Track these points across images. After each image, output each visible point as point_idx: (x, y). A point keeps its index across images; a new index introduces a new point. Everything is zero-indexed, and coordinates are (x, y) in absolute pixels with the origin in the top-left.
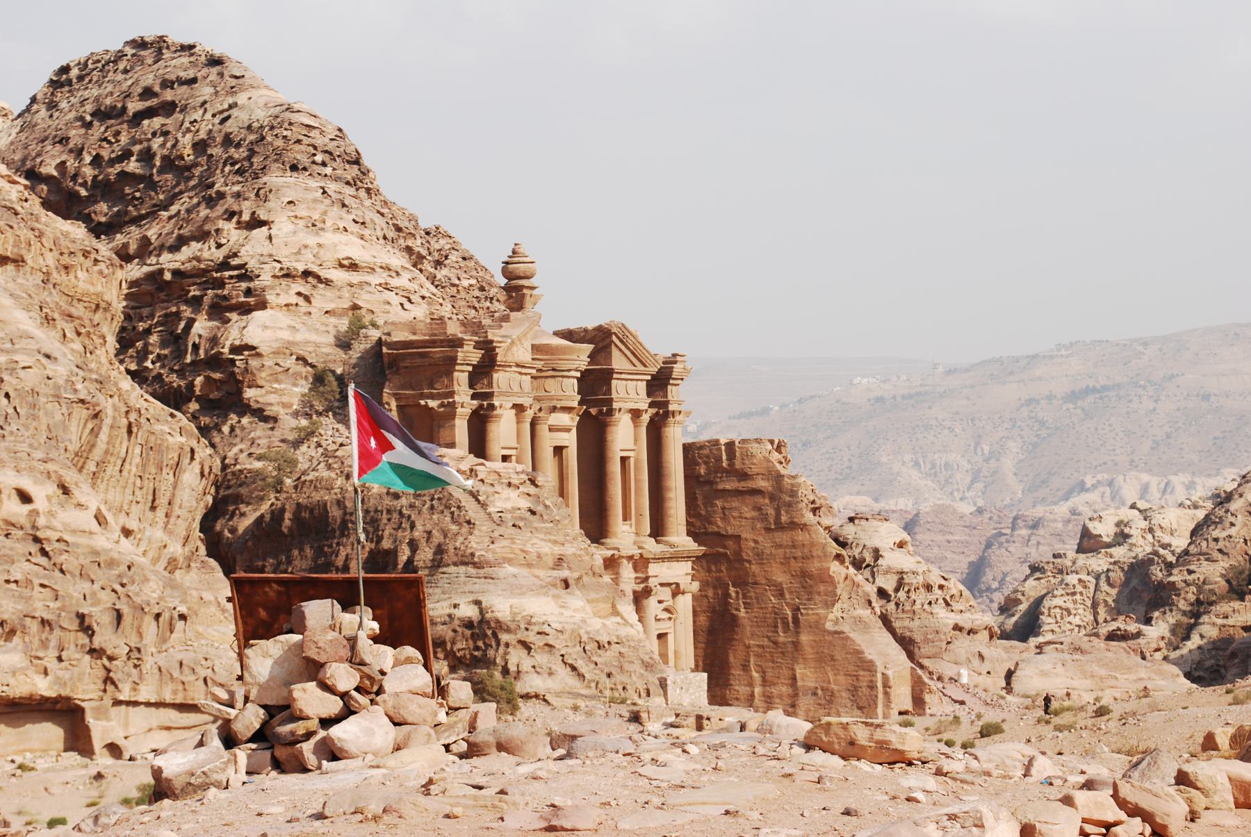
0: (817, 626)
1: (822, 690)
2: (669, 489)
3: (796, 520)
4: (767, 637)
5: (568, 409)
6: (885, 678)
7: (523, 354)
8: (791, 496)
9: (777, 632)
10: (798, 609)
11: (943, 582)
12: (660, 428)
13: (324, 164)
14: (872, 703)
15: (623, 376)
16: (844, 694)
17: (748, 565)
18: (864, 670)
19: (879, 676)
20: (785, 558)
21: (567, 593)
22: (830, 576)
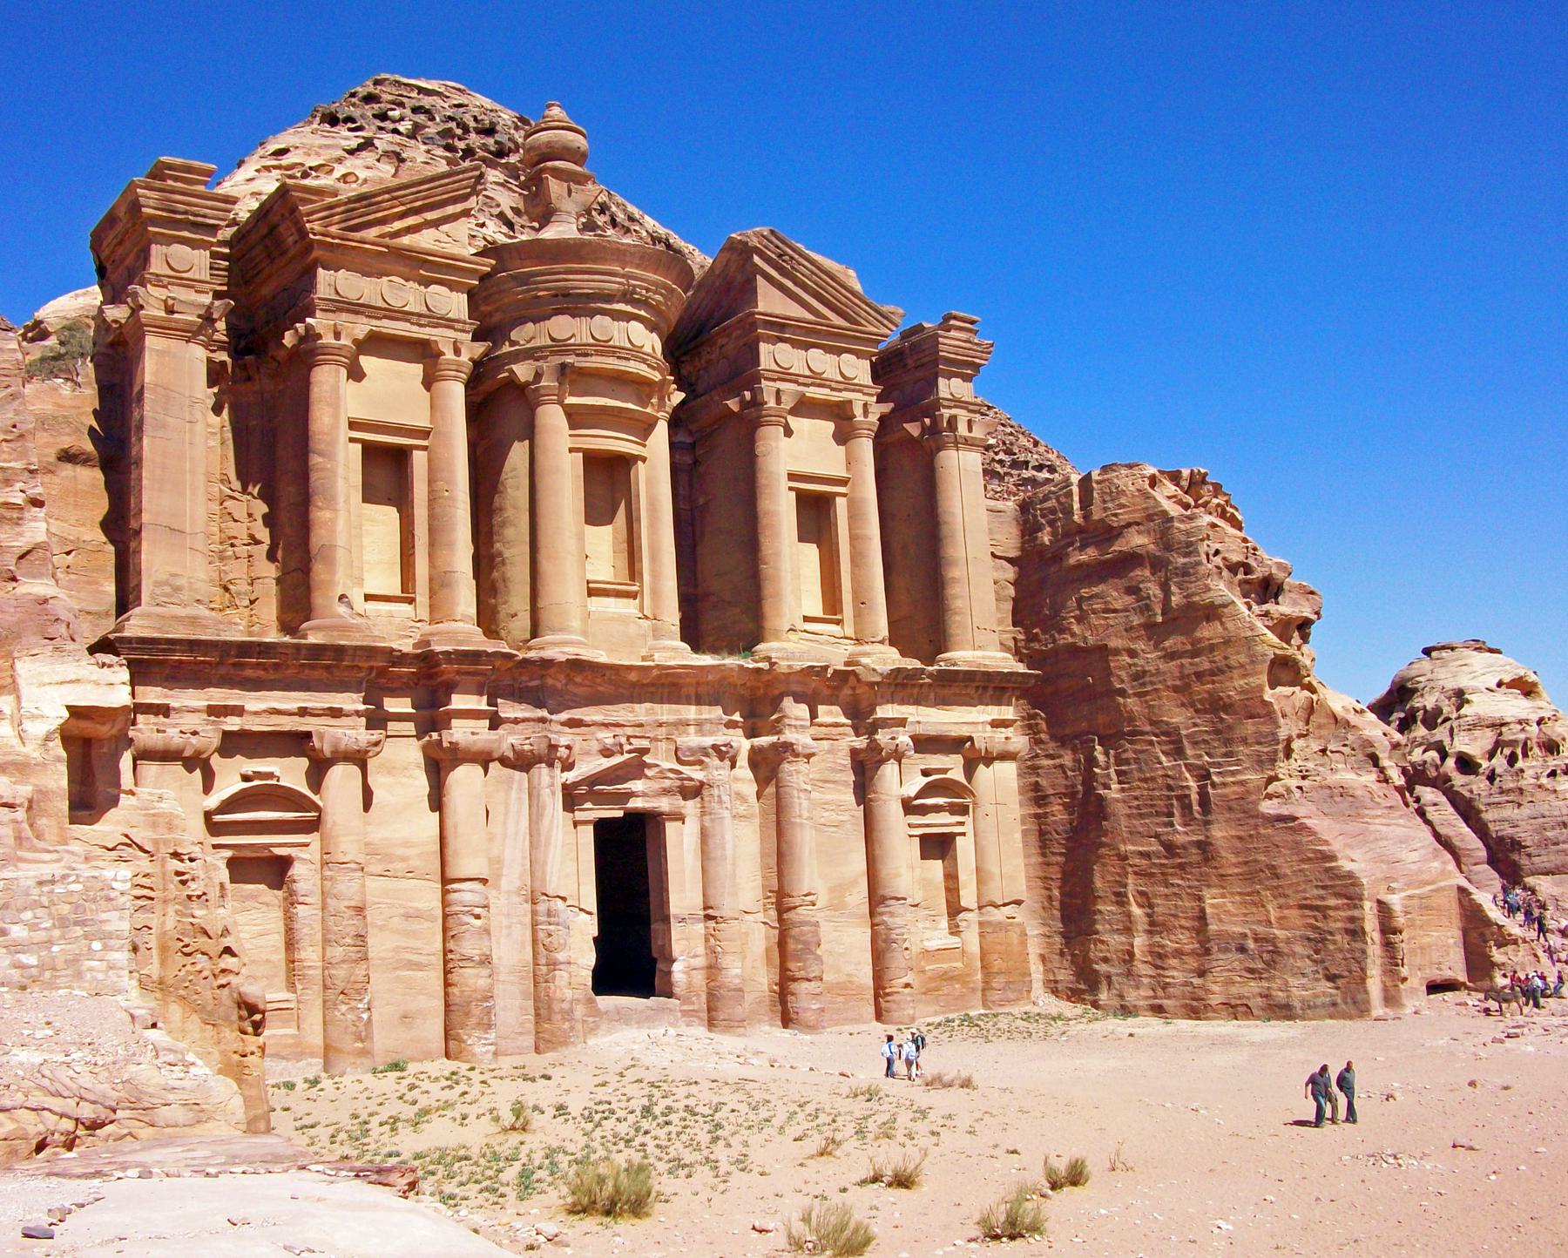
0: (1243, 808)
1: (1256, 940)
2: (952, 563)
3: (1197, 599)
4: (1157, 836)
5: (640, 387)
6: (1383, 908)
8: (1186, 555)
9: (1171, 824)
10: (1208, 776)
13: (402, 119)
14: (1355, 967)
16: (1299, 949)
17: (1121, 700)
18: (1338, 895)
19: (1369, 907)
20: (1182, 677)
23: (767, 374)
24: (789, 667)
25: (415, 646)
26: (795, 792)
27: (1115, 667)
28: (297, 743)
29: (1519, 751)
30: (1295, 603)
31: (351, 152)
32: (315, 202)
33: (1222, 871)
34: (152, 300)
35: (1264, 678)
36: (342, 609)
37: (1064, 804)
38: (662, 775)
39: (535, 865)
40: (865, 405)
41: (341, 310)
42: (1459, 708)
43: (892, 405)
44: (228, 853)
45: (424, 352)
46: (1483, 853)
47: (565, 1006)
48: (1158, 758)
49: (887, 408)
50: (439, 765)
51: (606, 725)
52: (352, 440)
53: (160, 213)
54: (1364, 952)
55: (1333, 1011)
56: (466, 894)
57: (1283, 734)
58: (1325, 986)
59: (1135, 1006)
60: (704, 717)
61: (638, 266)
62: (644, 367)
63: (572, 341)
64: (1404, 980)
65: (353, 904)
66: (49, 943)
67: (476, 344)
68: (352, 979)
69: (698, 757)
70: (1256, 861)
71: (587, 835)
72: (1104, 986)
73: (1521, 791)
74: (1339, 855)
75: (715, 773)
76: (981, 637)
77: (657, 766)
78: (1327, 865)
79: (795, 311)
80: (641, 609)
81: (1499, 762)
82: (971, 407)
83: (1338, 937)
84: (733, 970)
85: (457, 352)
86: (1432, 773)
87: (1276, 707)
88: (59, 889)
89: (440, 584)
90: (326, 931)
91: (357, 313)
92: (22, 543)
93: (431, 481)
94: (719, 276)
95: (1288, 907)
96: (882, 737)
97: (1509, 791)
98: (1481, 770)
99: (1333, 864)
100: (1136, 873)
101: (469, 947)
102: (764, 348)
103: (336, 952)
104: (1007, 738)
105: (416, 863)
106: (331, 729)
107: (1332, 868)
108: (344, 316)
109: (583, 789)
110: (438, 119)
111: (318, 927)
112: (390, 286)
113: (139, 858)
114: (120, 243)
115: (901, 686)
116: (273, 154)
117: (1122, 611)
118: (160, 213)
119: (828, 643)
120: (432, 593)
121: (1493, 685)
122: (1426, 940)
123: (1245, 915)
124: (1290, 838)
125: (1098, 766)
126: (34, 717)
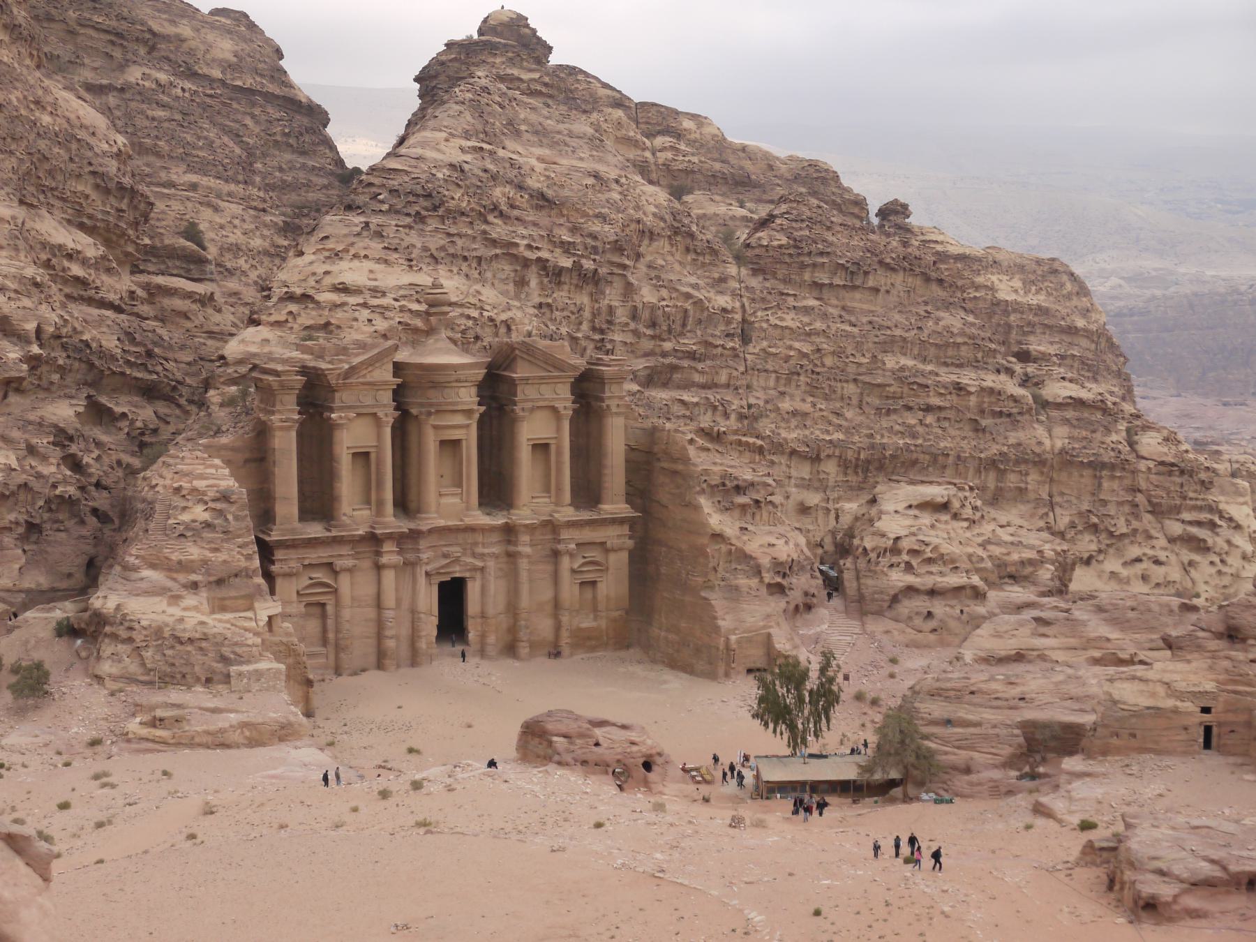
7: (385, 374)
11: (916, 547)
13: (382, 202)
21: (195, 594)
28: (330, 566)
30: (758, 492)
38: (467, 564)
50: (379, 568)
57: (711, 565)
69: (482, 556)
71: (435, 589)
73: (875, 572)
81: (873, 555)
89: (380, 504)
90: (336, 627)
96: (561, 547)
101: (388, 633)
115: (572, 524)
121: (901, 507)
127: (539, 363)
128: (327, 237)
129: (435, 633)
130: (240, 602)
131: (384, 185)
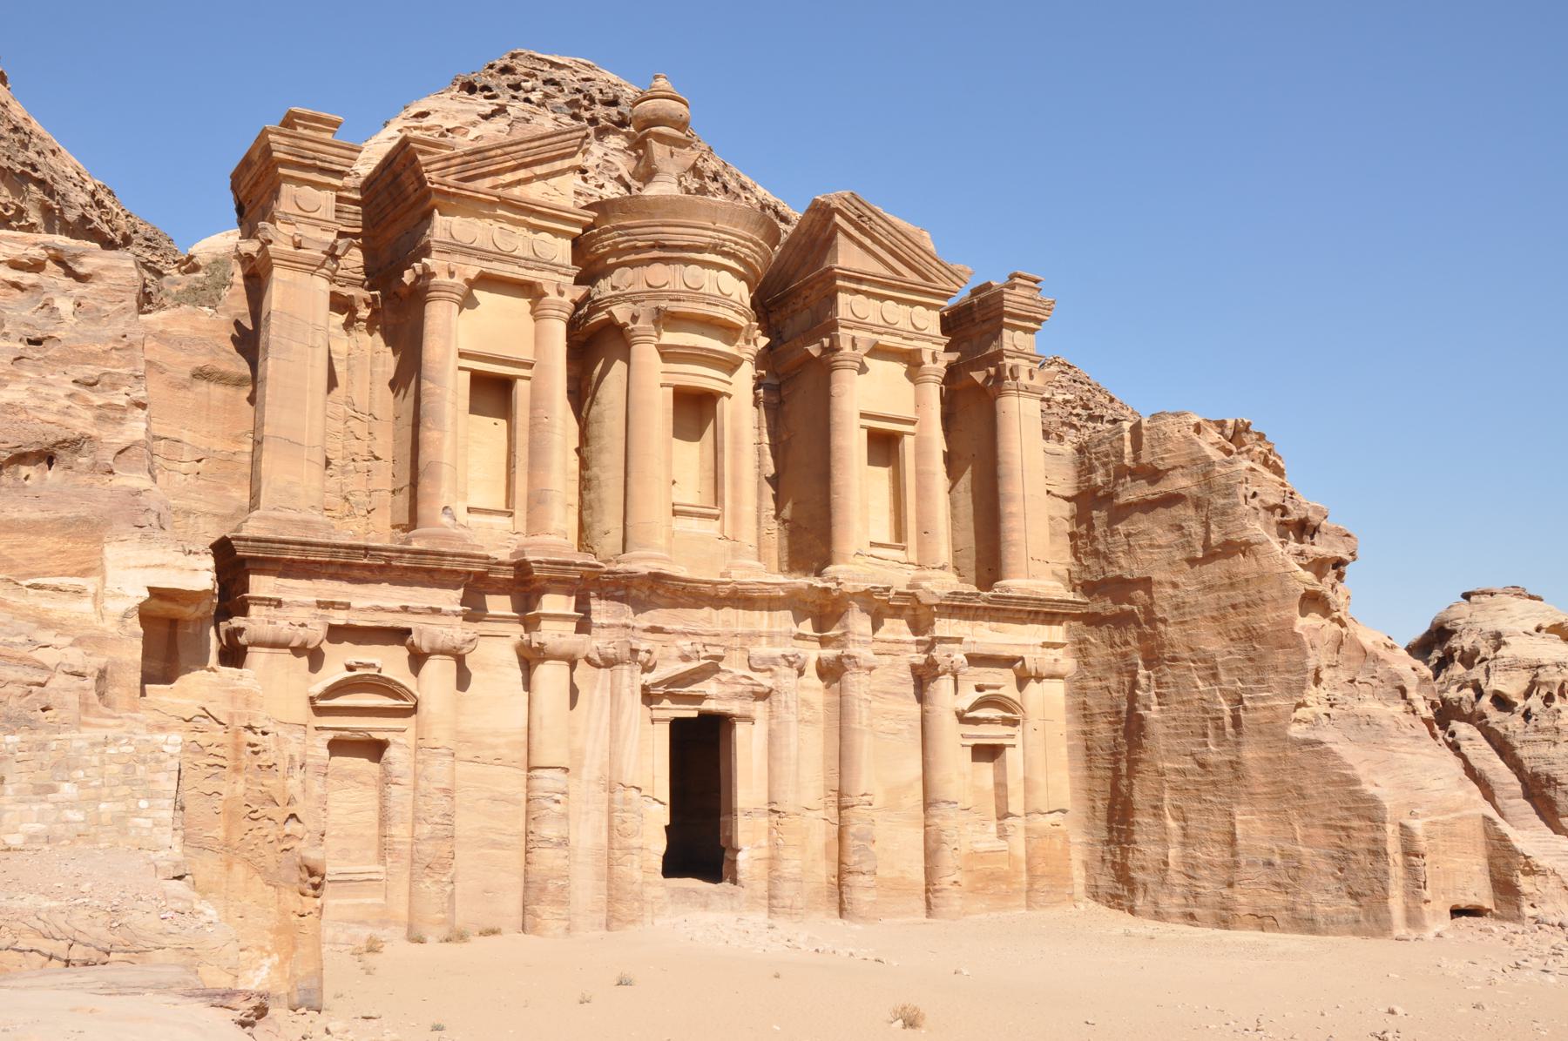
0: (1273, 732)
1: (1282, 856)
2: (1011, 499)
3: (1233, 537)
4: (1192, 754)
5: (728, 331)
8: (1227, 496)
9: (1207, 745)
10: (1241, 701)
12: (996, 399)
13: (534, 90)
14: (1377, 887)
15: (864, 288)
18: (1361, 817)
22: (1296, 636)
23: (844, 323)
24: (854, 587)
25: (512, 555)
26: (856, 702)
27: (1158, 598)
28: (399, 635)
29: (1555, 692)
30: (1331, 545)
31: (486, 117)
32: (433, 154)
33: (1251, 790)
34: (280, 236)
35: (1297, 611)
36: (445, 520)
37: (1110, 722)
39: (613, 756)
40: (934, 354)
41: (455, 252)
42: (1497, 649)
43: (958, 354)
44: (330, 735)
45: (529, 290)
46: (1518, 788)
47: (636, 888)
48: (1195, 683)
49: (954, 356)
50: (530, 659)
51: (685, 634)
52: (461, 368)
53: (290, 158)
54: (1386, 873)
55: (1356, 928)
56: (548, 781)
57: (1311, 664)
58: (1348, 903)
59: (1168, 913)
60: (775, 630)
61: (728, 222)
62: (732, 313)
63: (666, 288)
64: (1427, 901)
65: (443, 786)
66: (98, 799)
67: (578, 288)
68: (438, 854)
69: (768, 666)
70: (1283, 782)
72: (1140, 893)
74: (1363, 780)
75: (784, 681)
76: (1036, 567)
77: (730, 672)
78: (1351, 788)
79: (873, 267)
80: (722, 531)
81: (1535, 702)
82: (1032, 358)
83: (1361, 857)
84: (792, 865)
85: (561, 293)
86: (1467, 709)
87: (1305, 639)
88: (111, 750)
89: (537, 501)
90: (416, 810)
91: (470, 255)
92: (122, 440)
93: (533, 409)
94: (804, 234)
95: (1313, 826)
96: (939, 653)
97: (1544, 731)
98: (1516, 709)
99: (1357, 788)
100: (1172, 789)
101: (549, 830)
102: (842, 298)
103: (425, 830)
104: (1056, 660)
105: (503, 751)
106: (429, 627)
107: (1356, 791)
108: (458, 258)
109: (661, 690)
110: (566, 91)
111: (409, 807)
112: (501, 233)
113: (217, 730)
114: (256, 184)
116: (416, 116)
117: (1167, 547)
118: (290, 158)
119: (892, 567)
120: (530, 510)
121: (1532, 629)
122: (1449, 865)
123: (1272, 832)
124: (1316, 761)
125: (1140, 689)
126: (115, 596)
127: (876, 248)
128: (424, 115)
129: (660, 845)
130: (48, 543)
131: (535, 75)
